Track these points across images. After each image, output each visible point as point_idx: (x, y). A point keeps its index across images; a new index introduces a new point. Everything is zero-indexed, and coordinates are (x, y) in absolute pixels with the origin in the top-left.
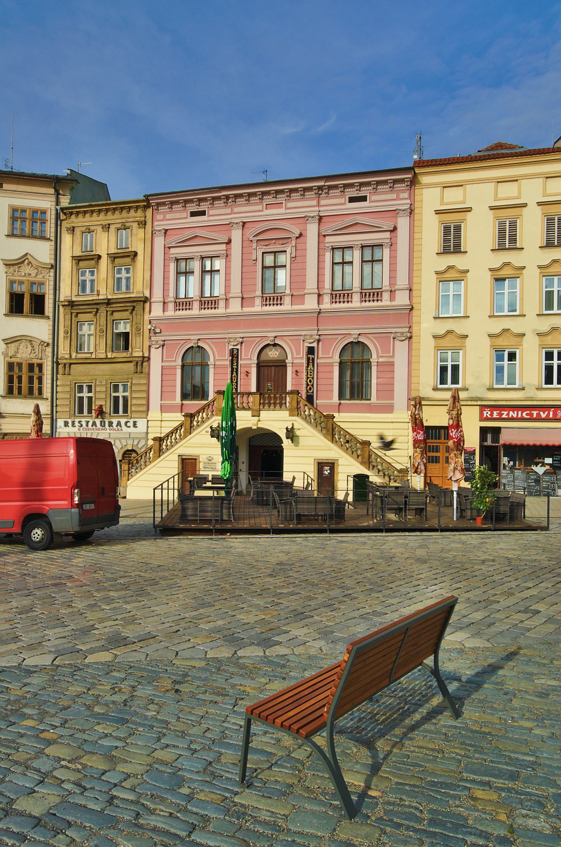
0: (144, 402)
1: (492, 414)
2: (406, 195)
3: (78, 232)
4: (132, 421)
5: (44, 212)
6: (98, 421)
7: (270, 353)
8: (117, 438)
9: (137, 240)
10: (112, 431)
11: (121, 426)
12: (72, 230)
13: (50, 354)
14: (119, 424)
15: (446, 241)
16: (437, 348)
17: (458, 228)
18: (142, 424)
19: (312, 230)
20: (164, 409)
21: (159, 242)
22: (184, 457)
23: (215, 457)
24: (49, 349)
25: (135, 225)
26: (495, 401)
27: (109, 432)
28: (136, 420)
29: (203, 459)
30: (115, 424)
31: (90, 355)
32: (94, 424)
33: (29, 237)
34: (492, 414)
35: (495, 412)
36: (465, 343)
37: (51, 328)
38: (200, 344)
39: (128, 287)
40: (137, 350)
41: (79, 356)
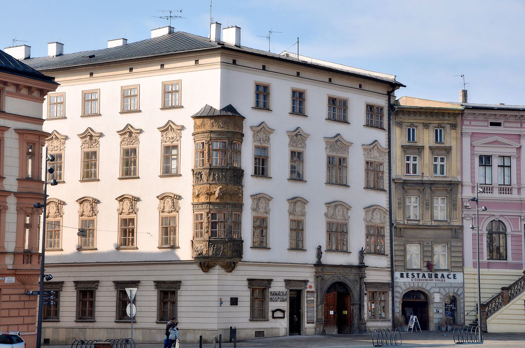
0: (461, 260)
4: (452, 274)
5: (382, 109)
6: (426, 274)
8: (441, 287)
10: (437, 282)
11: (444, 278)
12: (400, 124)
13: (388, 220)
14: (443, 276)
18: (459, 275)
21: (467, 141)
24: (388, 217)
25: (448, 127)
27: (436, 282)
28: (455, 273)
30: (439, 276)
31: (418, 222)
32: (424, 276)
33: (375, 127)
37: (388, 199)
38: (502, 219)
39: (442, 173)
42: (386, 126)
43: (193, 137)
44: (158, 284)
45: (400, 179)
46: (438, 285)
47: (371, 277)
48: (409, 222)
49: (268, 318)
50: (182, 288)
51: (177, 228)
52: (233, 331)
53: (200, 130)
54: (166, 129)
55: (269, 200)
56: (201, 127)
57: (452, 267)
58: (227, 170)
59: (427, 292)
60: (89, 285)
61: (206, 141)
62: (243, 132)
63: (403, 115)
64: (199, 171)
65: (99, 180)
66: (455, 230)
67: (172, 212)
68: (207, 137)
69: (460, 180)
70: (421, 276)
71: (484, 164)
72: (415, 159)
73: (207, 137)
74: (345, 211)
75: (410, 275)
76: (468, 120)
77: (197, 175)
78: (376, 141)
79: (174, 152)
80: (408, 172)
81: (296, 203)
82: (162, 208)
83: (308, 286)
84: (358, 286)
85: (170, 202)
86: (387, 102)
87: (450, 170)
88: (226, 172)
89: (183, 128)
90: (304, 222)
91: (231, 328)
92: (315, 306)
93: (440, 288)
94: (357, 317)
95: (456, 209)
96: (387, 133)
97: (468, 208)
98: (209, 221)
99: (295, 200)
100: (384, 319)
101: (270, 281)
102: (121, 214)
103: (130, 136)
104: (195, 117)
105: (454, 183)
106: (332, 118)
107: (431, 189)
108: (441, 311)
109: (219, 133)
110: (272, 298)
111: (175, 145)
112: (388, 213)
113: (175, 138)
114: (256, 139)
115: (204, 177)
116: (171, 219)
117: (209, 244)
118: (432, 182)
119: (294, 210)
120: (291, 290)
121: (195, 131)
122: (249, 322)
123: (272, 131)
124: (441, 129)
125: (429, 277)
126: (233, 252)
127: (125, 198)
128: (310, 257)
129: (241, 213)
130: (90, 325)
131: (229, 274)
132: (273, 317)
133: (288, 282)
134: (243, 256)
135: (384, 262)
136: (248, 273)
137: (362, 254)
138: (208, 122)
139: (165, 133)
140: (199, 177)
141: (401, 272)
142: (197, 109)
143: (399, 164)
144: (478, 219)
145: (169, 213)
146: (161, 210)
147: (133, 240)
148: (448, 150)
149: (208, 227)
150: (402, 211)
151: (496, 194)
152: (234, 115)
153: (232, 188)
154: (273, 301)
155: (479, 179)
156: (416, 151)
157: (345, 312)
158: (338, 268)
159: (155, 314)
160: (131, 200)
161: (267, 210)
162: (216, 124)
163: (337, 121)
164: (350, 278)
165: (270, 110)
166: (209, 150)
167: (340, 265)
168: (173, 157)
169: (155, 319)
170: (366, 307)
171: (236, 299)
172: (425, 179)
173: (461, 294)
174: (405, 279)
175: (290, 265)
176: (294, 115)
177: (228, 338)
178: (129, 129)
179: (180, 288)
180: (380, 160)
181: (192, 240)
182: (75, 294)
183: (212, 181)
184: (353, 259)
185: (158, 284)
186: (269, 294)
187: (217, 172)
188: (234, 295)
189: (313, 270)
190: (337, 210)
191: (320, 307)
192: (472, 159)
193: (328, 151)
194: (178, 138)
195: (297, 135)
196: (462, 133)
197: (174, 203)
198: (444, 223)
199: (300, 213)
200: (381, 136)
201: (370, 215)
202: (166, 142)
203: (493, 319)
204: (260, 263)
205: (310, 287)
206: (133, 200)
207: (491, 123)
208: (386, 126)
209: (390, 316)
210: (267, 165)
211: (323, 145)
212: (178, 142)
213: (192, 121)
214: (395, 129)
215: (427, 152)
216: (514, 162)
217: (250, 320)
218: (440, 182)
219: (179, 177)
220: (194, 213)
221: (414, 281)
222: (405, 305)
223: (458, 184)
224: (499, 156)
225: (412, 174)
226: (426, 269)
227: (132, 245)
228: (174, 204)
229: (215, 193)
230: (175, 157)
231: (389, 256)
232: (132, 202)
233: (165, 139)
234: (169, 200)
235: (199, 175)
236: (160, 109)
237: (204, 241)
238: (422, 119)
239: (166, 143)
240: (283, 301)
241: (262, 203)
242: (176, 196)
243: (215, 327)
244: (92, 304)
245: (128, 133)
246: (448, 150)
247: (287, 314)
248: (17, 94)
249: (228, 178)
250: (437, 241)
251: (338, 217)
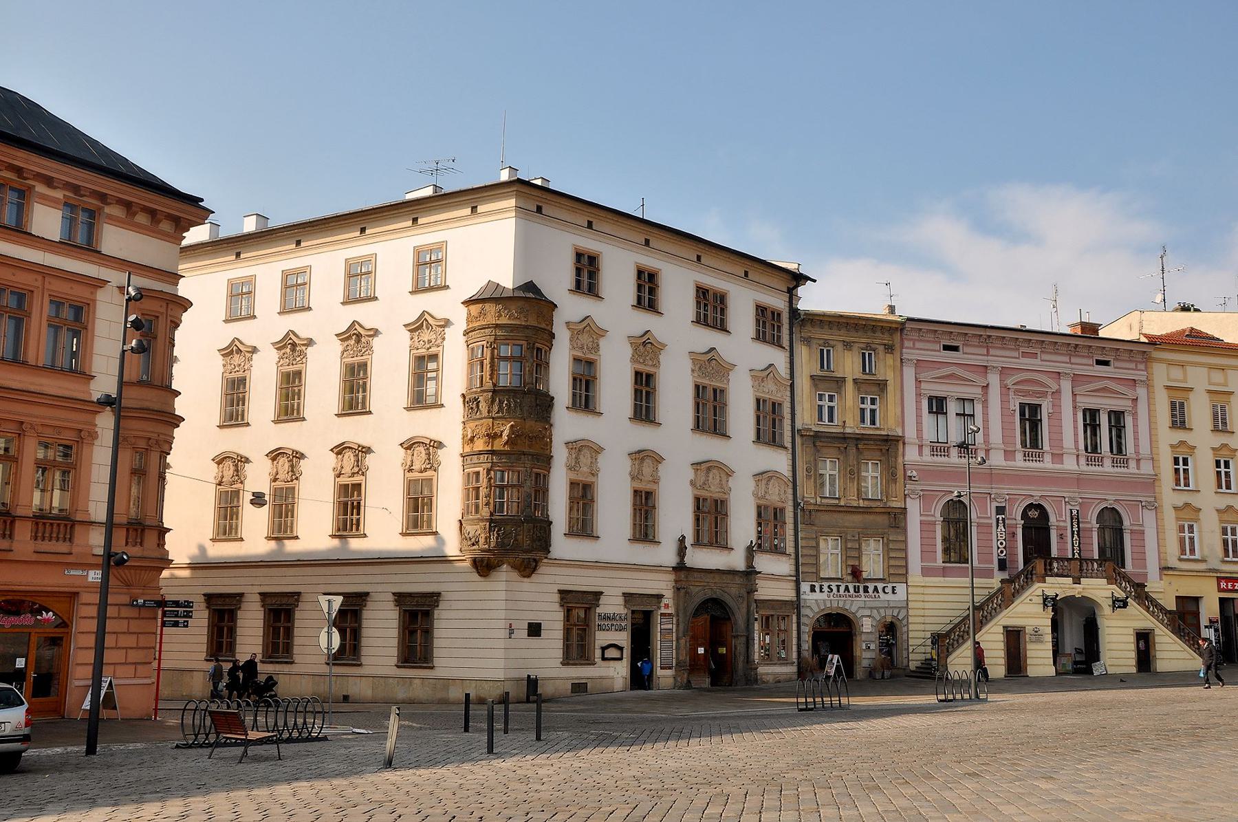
1: (1227, 586)
2: (1142, 366)
3: (814, 343)
7: (1030, 513)
9: (885, 366)
10: (867, 599)
11: (878, 592)
12: (807, 341)
13: (791, 497)
14: (876, 589)
15: (1173, 416)
16: (1178, 519)
17: (1182, 405)
18: (901, 588)
19: (1066, 385)
20: (926, 572)
21: (909, 373)
22: (1009, 629)
23: (1041, 628)
24: (790, 491)
25: (882, 348)
26: (1197, 572)
28: (894, 585)
29: (1029, 630)
30: (871, 589)
31: (837, 502)
32: (847, 589)
34: (1227, 586)
35: (1229, 584)
36: (1198, 515)
39: (873, 422)
40: (894, 499)
41: (824, 501)
42: (786, 343)
43: (465, 338)
44: (400, 598)
45: (810, 430)
46: (869, 604)
47: (766, 590)
48: (824, 501)
49: (594, 660)
50: (442, 605)
51: (434, 499)
52: (532, 683)
53: (476, 324)
54: (418, 326)
55: (597, 452)
56: (478, 319)
57: (890, 575)
58: (525, 393)
59: (851, 616)
60: (285, 600)
61: (488, 342)
63: (813, 326)
64: (474, 396)
65: (304, 419)
66: (895, 515)
67: (425, 470)
68: (490, 335)
69: (901, 435)
70: (842, 589)
71: (934, 410)
72: (831, 398)
73: (490, 335)
74: (724, 477)
75: (825, 589)
76: (912, 339)
77: (470, 402)
78: (771, 365)
79: (432, 366)
80: (820, 419)
81: (643, 459)
82: (409, 463)
83: (662, 605)
84: (745, 605)
85: (424, 452)
86: (787, 304)
87: (885, 418)
88: (523, 398)
89: (447, 323)
90: (657, 494)
91: (529, 676)
92: (674, 639)
93: (871, 608)
94: (742, 658)
95: (895, 481)
96: (788, 354)
97: (913, 479)
98: (490, 484)
99: (642, 455)
100: (785, 662)
101: (598, 595)
102: (339, 476)
103: (358, 341)
104: (468, 303)
105: (893, 438)
106: (702, 320)
107: (857, 448)
108: (873, 647)
109: (510, 329)
111: (434, 353)
112: (791, 485)
113: (433, 341)
114: (576, 346)
115: (483, 406)
116: (424, 483)
117: (490, 525)
118: (859, 436)
119: (640, 472)
120: (633, 612)
121: (470, 326)
122: (561, 666)
123: (602, 333)
124: (871, 352)
125: (855, 592)
126: (533, 541)
127: (346, 448)
128: (666, 555)
129: (549, 472)
130: (286, 668)
131: (526, 580)
132: (604, 659)
133: (628, 597)
134: (551, 549)
135: (783, 566)
136: (559, 579)
137: (750, 552)
138: (491, 308)
139: (417, 333)
140: (474, 406)
141: (811, 583)
142: (472, 291)
143: (807, 405)
144: (926, 498)
145: (421, 472)
146: (407, 467)
147: (358, 520)
148: (882, 386)
149: (488, 496)
150: (813, 483)
151: (954, 457)
152: (538, 297)
153: (532, 425)
154: (604, 630)
155: (929, 435)
156: (834, 385)
157: (723, 650)
158: (712, 575)
159: (395, 652)
160: (357, 451)
161: (594, 469)
162: (506, 312)
163: (711, 326)
164: (731, 592)
165: (600, 297)
166: (492, 358)
167: (716, 569)
168: (430, 375)
169: (394, 661)
170: (756, 642)
172: (848, 430)
173: (903, 619)
174: (817, 595)
175: (633, 567)
176: (640, 309)
177: (523, 696)
178: (356, 329)
179: (438, 606)
180: (777, 398)
181: (461, 519)
182: (261, 615)
183: (498, 413)
184: (736, 560)
185: (400, 598)
186: (597, 617)
187: (507, 397)
188: (535, 618)
189: (672, 577)
190: (711, 475)
191: (682, 641)
192: (918, 402)
194: (439, 341)
195: (644, 344)
196: (901, 359)
197: (429, 454)
198: (878, 504)
199: (651, 479)
200: (779, 358)
201: (764, 487)
202: (418, 349)
203: (957, 657)
204: (581, 563)
205: (667, 606)
206: (359, 451)
207: (944, 345)
208: (786, 343)
209: (795, 655)
210: (595, 391)
211: (688, 365)
212: (439, 349)
213: (464, 310)
214: (800, 349)
215: (849, 386)
216: (979, 408)
217: (563, 664)
218: (871, 437)
219: (439, 409)
220: (465, 471)
221: (832, 598)
222: (817, 636)
223: (898, 441)
224: (957, 398)
225: (827, 423)
226: (850, 578)
227: (357, 529)
228: (429, 456)
229: (501, 435)
230: (434, 374)
231: (793, 556)
232: (357, 455)
233: (416, 344)
234: (422, 449)
235: (475, 403)
236: (410, 292)
237: (482, 520)
238: (842, 335)
239: (418, 351)
240: (620, 630)
242: (433, 442)
243: (501, 675)
244: (289, 633)
245: (354, 337)
246: (882, 386)
247: (627, 653)
248: (128, 223)
249: (526, 408)
250: (865, 533)
251: (713, 488)
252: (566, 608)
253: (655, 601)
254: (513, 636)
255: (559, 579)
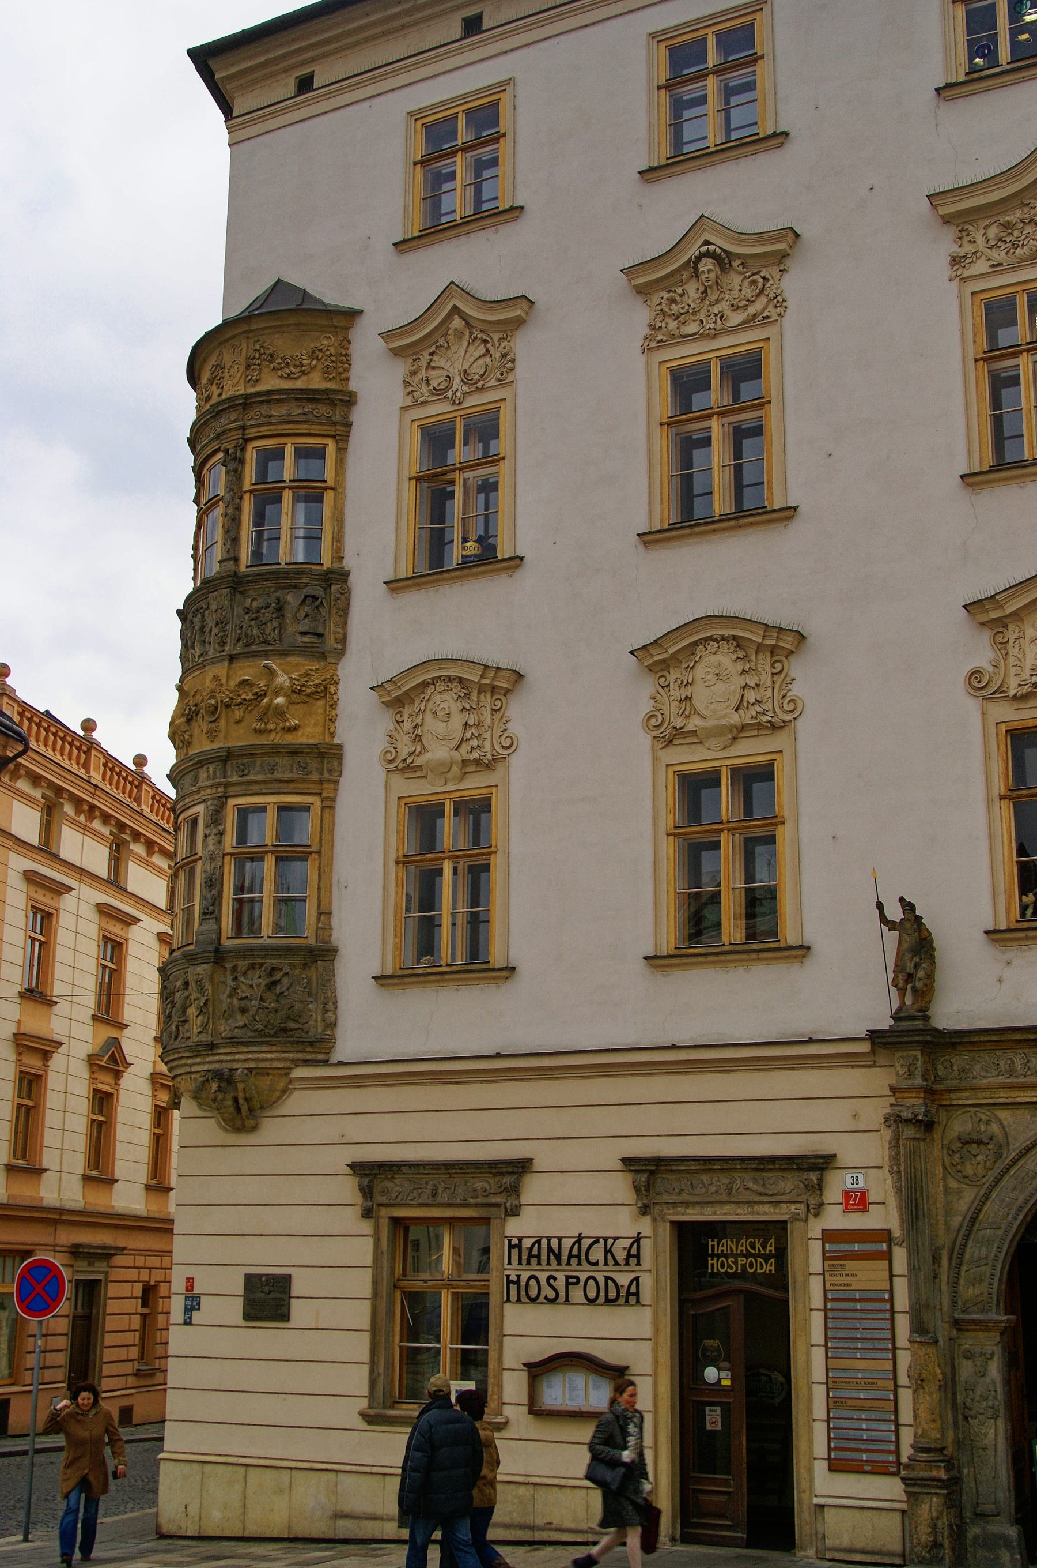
62: (353, 386)
110: (518, 1282)
122: (364, 1426)
132: (536, 1410)
136: (356, 1129)
154: (533, 1300)
171: (285, 1281)
193: (981, 266)
205: (858, 1201)
240: (608, 1301)
241: (440, 714)
252: (384, 1223)
253: (788, 1183)
254: (196, 1317)
255: (356, 1129)
